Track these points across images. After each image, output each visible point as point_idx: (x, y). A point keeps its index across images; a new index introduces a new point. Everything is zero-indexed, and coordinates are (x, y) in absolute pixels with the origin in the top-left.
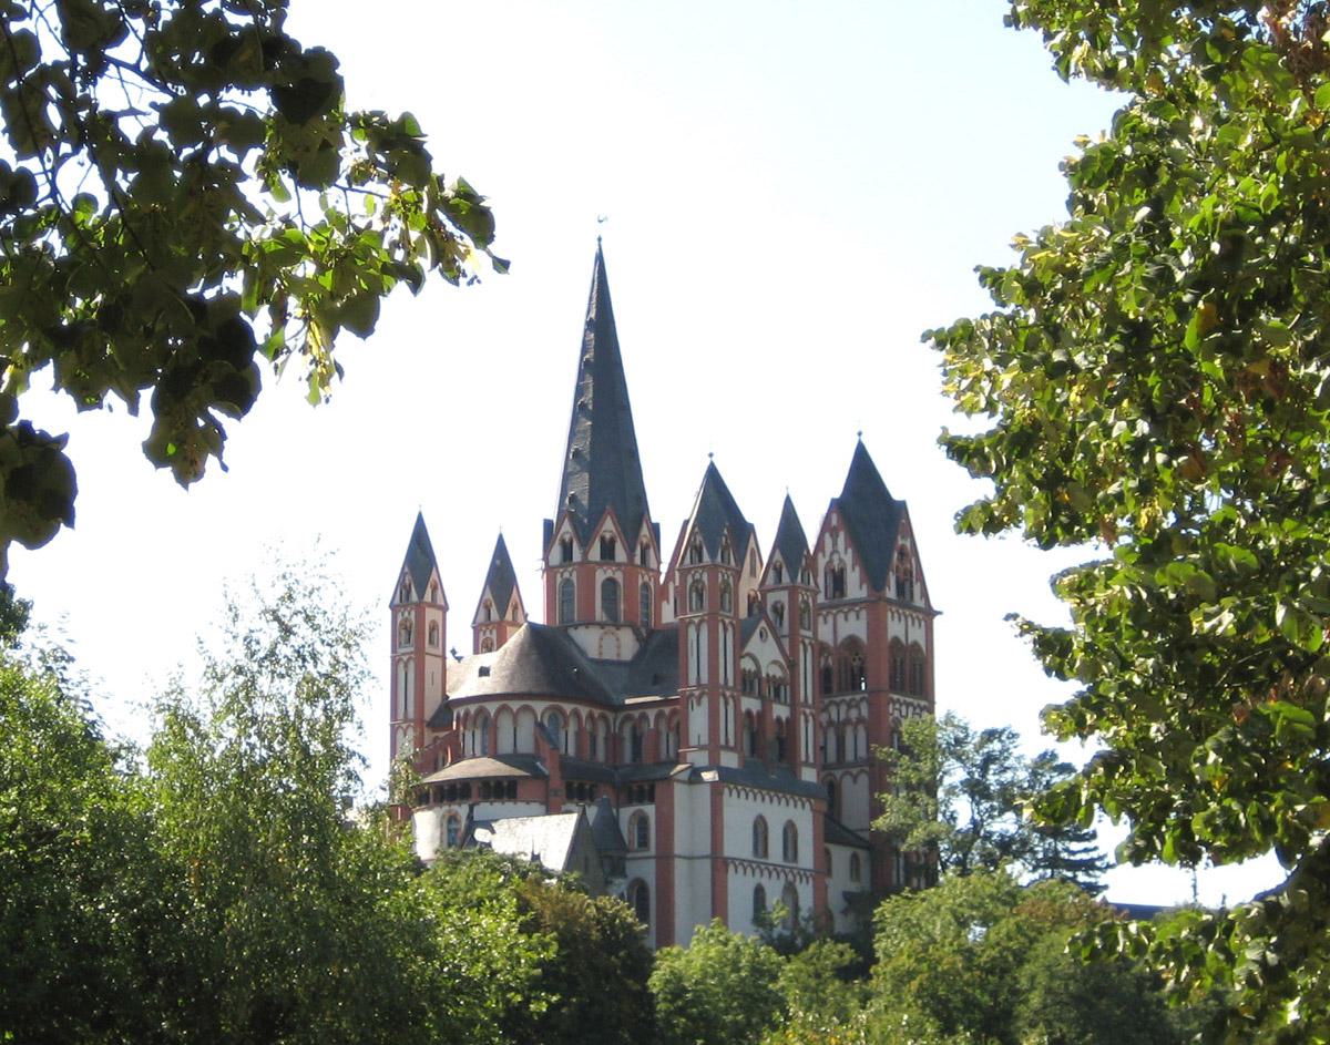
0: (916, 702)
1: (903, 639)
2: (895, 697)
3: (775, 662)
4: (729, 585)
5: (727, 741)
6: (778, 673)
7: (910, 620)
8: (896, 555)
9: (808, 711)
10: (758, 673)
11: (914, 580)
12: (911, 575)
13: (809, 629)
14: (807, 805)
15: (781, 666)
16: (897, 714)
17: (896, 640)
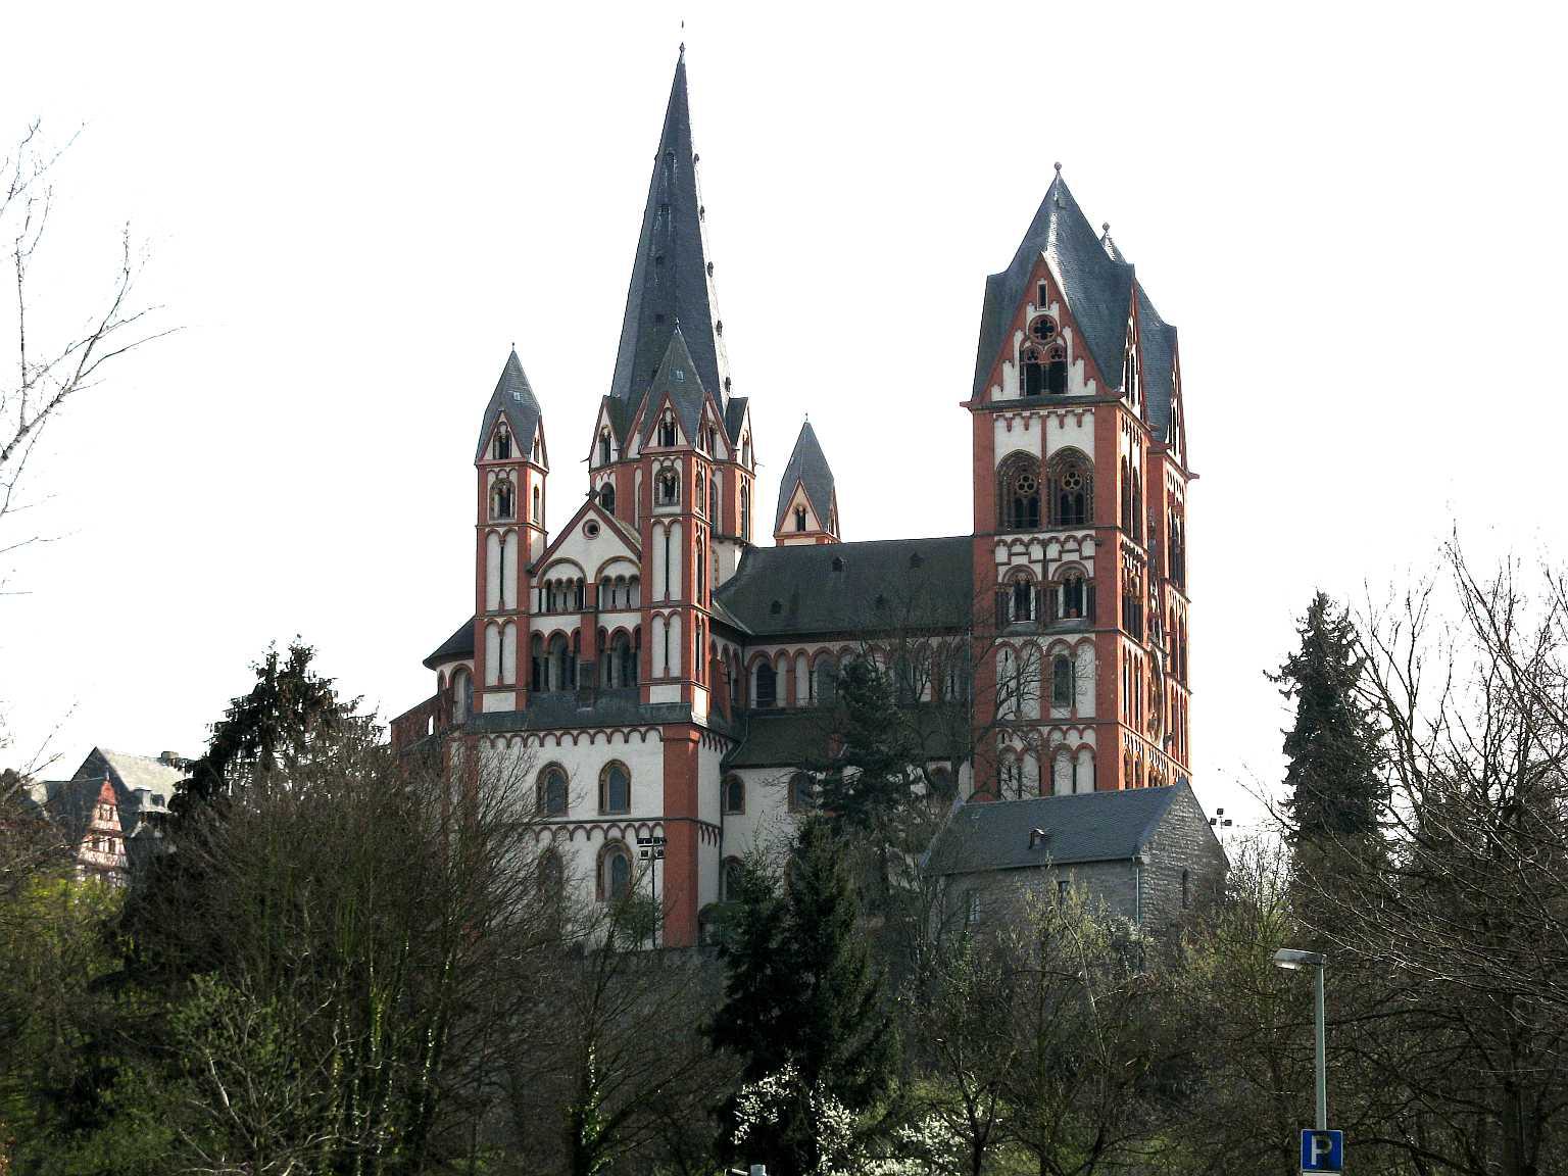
0: (1062, 536)
1: (1036, 451)
2: (1009, 538)
3: (616, 560)
4: (510, 482)
5: (501, 677)
6: (627, 570)
7: (1053, 422)
8: (1019, 336)
9: (666, 611)
10: (582, 581)
11: (1070, 359)
12: (1066, 357)
13: (678, 503)
14: (653, 736)
15: (631, 561)
16: (1023, 560)
17: (1019, 458)
